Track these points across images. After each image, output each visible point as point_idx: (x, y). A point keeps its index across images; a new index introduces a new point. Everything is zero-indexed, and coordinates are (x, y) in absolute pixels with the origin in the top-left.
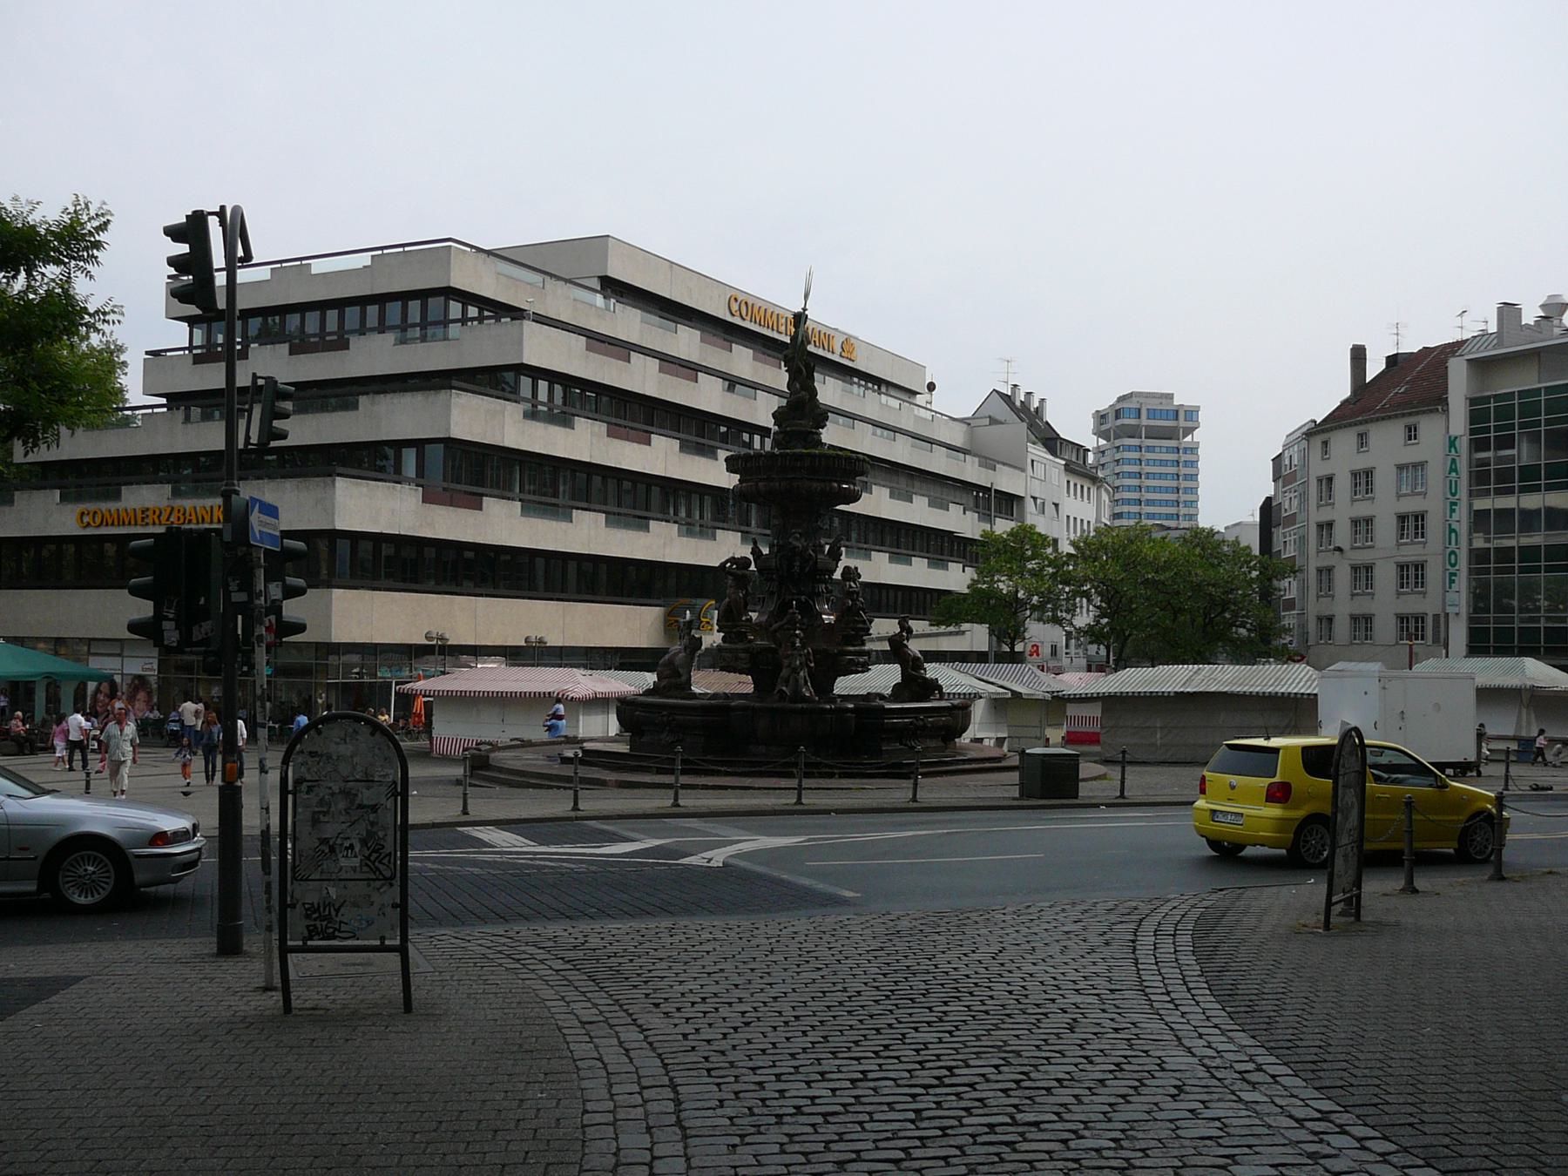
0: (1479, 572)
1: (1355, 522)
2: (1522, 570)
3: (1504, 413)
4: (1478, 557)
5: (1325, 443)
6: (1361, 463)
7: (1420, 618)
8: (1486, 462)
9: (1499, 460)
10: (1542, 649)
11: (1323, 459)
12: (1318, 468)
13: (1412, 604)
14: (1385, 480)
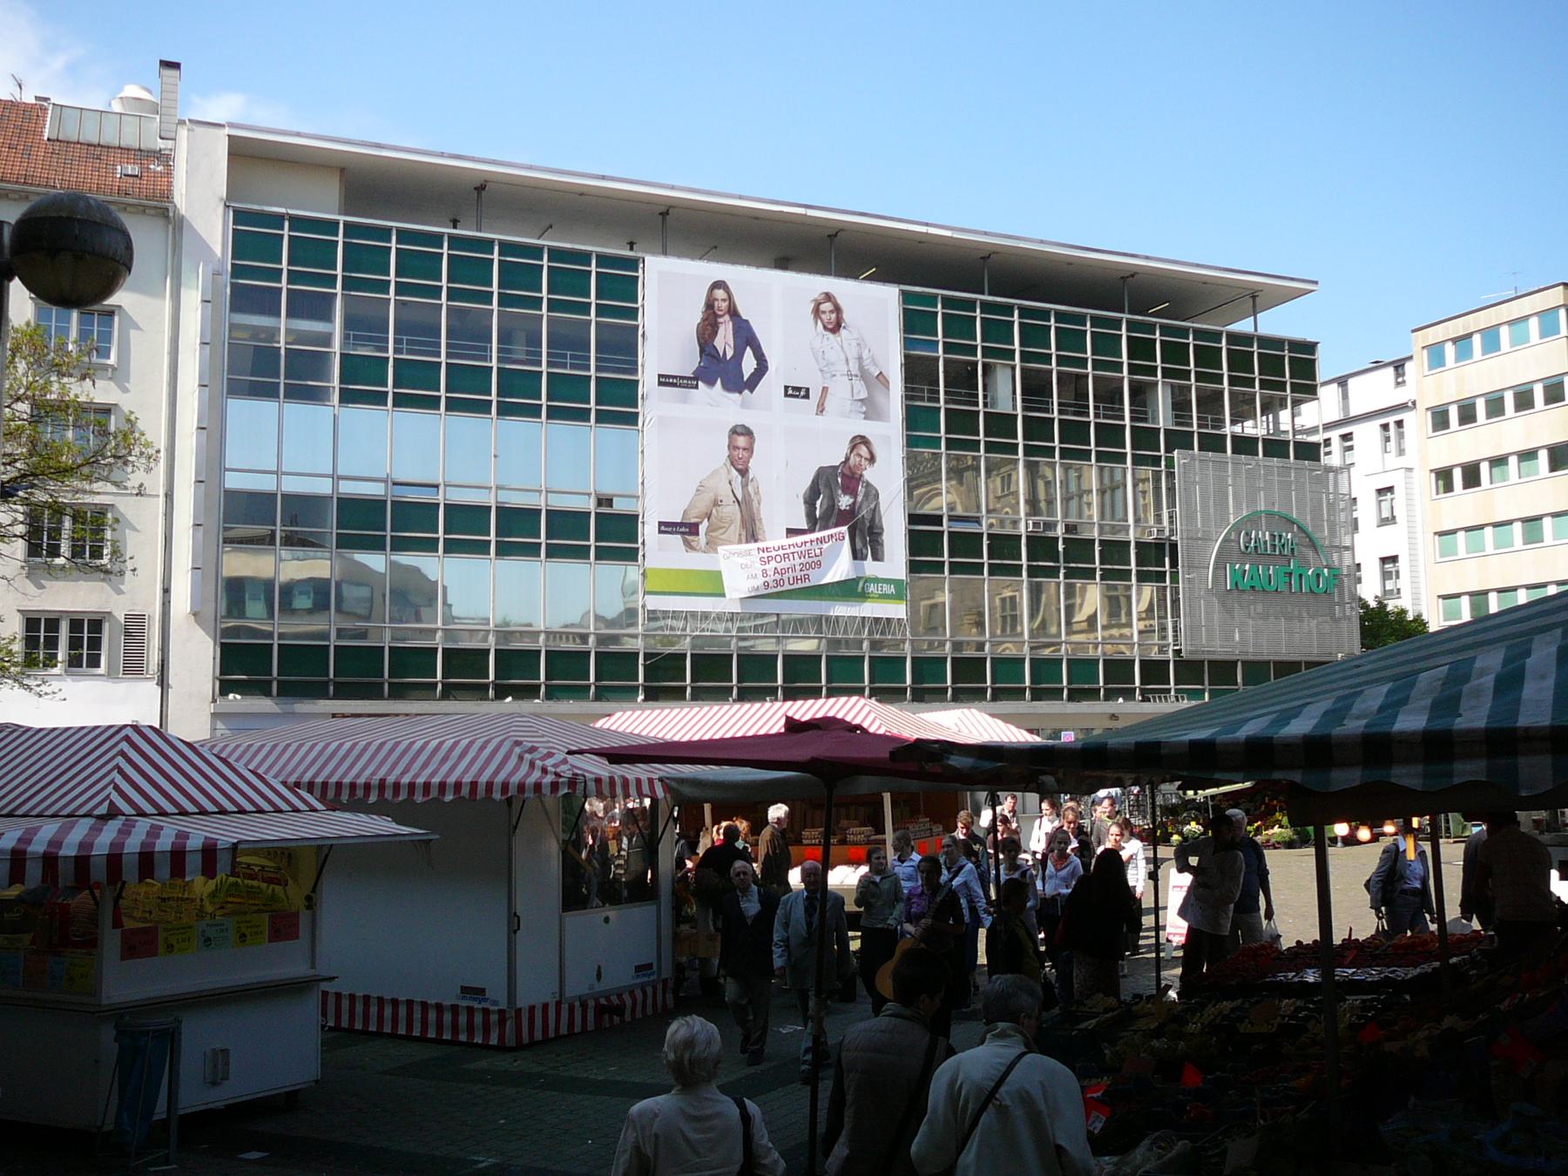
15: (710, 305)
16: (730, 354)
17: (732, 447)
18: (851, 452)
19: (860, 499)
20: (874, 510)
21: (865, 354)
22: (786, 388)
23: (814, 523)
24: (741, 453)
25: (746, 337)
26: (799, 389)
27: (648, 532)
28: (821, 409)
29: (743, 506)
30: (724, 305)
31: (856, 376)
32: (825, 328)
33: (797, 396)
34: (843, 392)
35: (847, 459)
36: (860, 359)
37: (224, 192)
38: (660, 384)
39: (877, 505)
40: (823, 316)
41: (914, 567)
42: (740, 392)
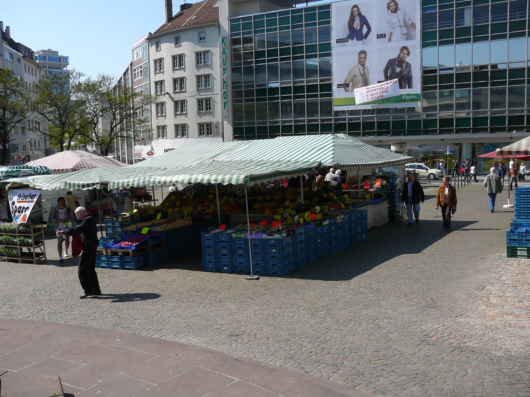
0: (236, 101)
1: (175, 81)
2: (258, 100)
7: (209, 125)
10: (245, 137)
12: (154, 55)
13: (206, 119)
15: (352, 14)
16: (358, 28)
17: (360, 58)
18: (401, 52)
19: (404, 68)
20: (409, 71)
21: (407, 17)
22: (377, 35)
23: (387, 78)
24: (362, 60)
25: (364, 21)
26: (382, 35)
27: (334, 87)
28: (390, 40)
29: (363, 76)
30: (356, 13)
31: (403, 26)
32: (392, 12)
33: (381, 38)
34: (397, 32)
35: (399, 55)
36: (404, 20)
37: (228, 16)
38: (337, 42)
39: (410, 69)
40: (391, 8)
41: (424, 89)
42: (362, 40)
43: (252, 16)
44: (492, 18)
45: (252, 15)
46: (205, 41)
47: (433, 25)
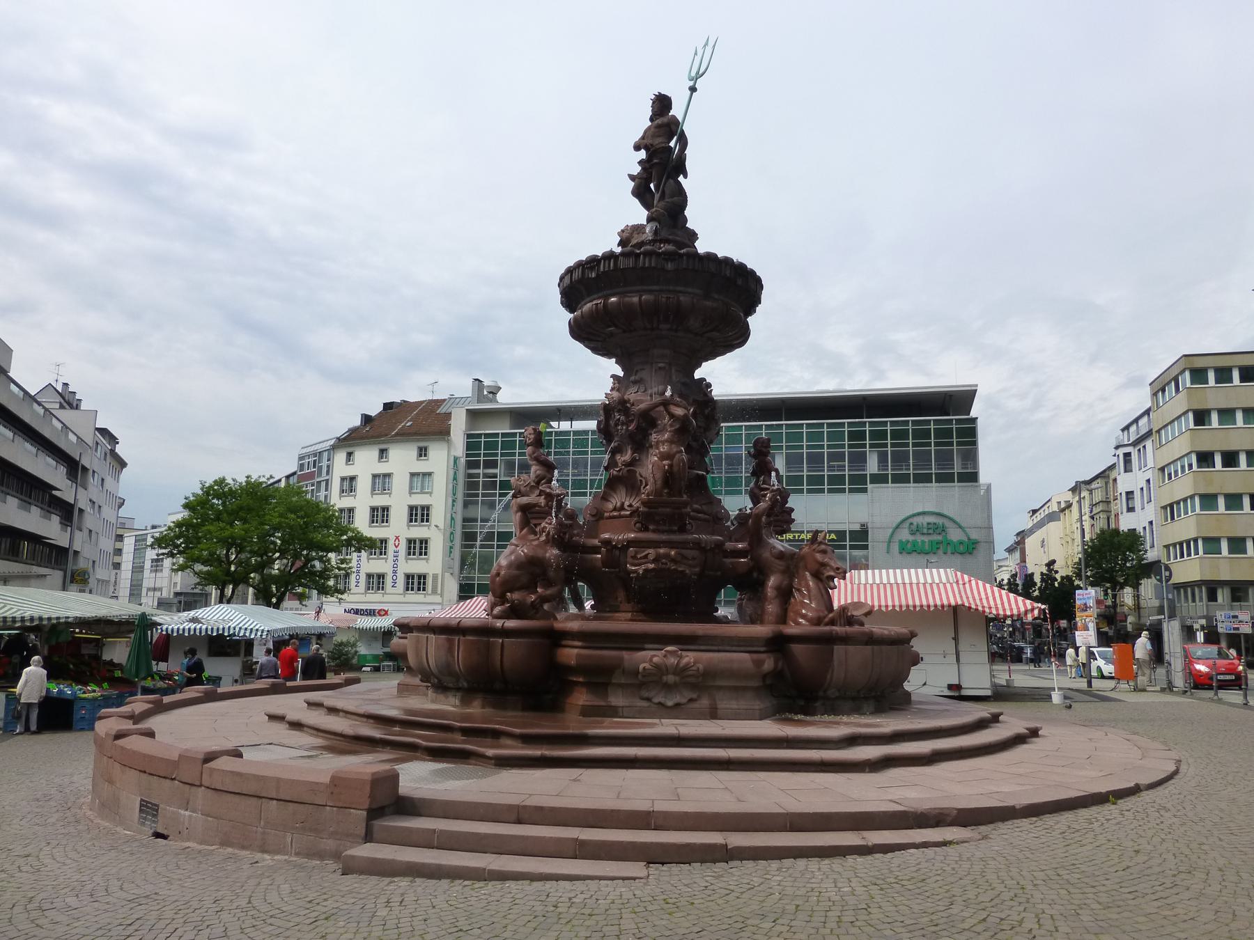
3: (491, 446)
4: (469, 537)
5: (350, 455)
6: (382, 468)
7: (422, 577)
8: (478, 476)
9: (485, 476)
11: (347, 464)
14: (400, 483)
43: (499, 433)
44: (808, 467)
45: (500, 432)
46: (427, 460)
47: (738, 469)
